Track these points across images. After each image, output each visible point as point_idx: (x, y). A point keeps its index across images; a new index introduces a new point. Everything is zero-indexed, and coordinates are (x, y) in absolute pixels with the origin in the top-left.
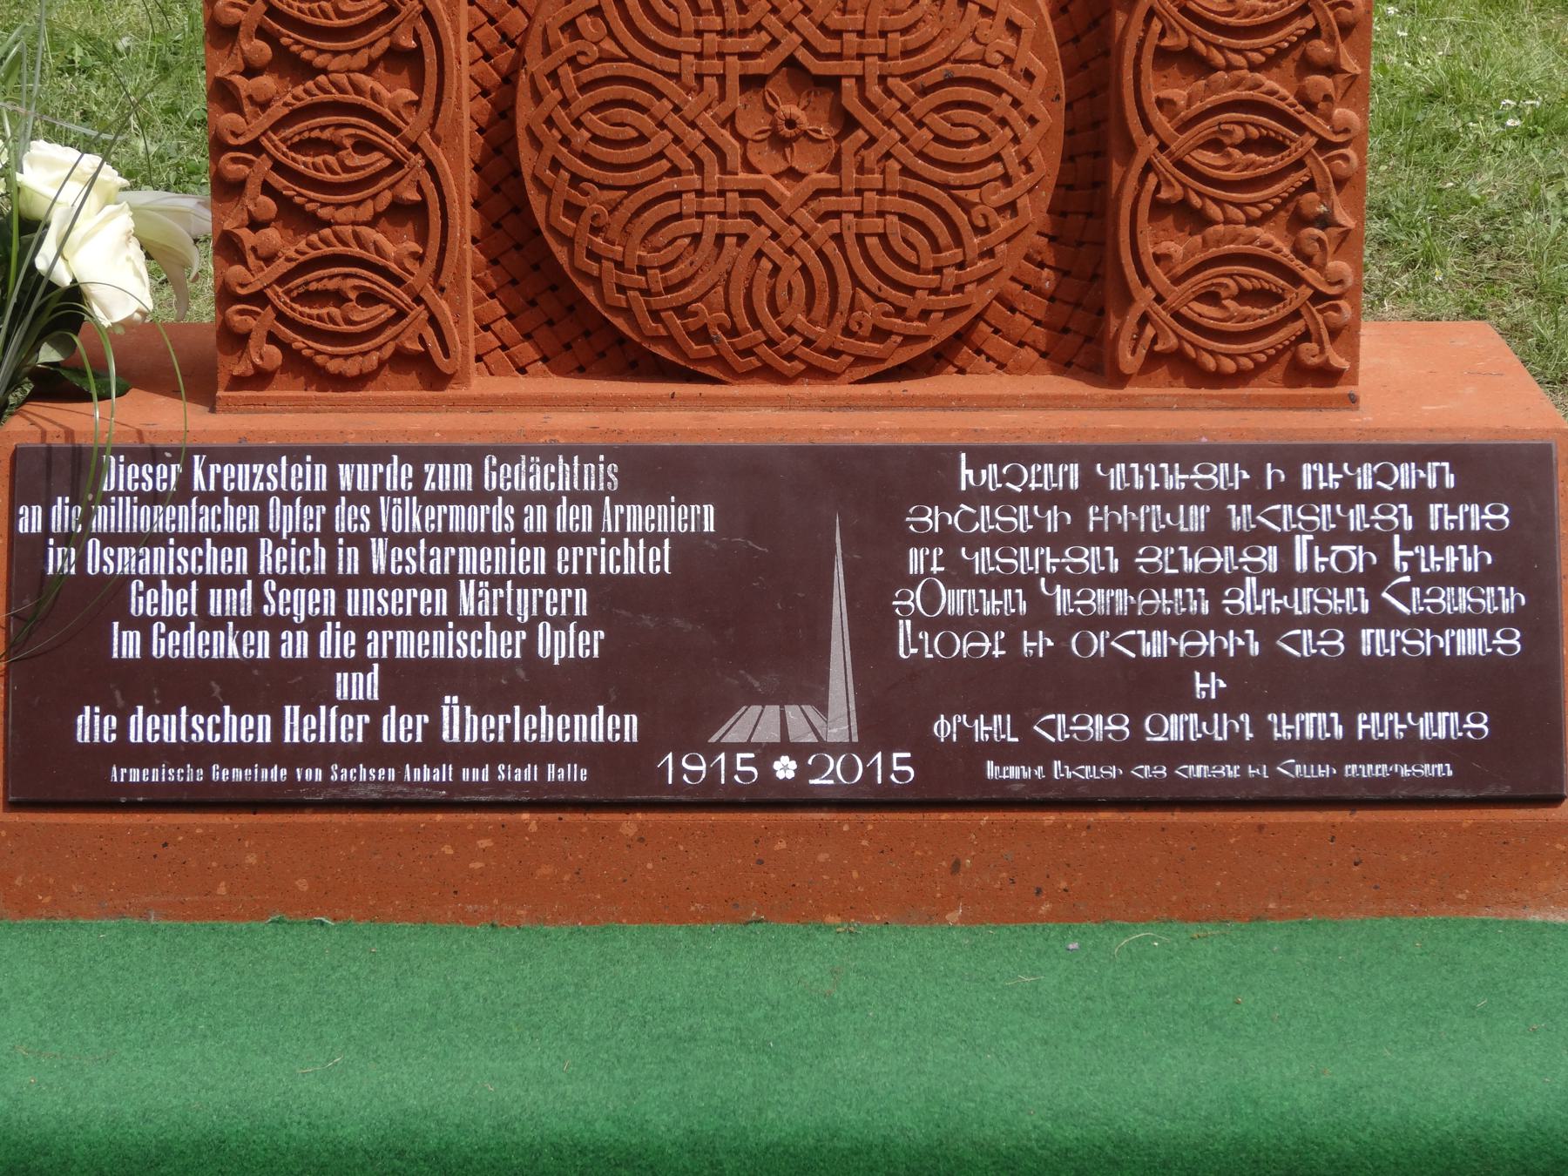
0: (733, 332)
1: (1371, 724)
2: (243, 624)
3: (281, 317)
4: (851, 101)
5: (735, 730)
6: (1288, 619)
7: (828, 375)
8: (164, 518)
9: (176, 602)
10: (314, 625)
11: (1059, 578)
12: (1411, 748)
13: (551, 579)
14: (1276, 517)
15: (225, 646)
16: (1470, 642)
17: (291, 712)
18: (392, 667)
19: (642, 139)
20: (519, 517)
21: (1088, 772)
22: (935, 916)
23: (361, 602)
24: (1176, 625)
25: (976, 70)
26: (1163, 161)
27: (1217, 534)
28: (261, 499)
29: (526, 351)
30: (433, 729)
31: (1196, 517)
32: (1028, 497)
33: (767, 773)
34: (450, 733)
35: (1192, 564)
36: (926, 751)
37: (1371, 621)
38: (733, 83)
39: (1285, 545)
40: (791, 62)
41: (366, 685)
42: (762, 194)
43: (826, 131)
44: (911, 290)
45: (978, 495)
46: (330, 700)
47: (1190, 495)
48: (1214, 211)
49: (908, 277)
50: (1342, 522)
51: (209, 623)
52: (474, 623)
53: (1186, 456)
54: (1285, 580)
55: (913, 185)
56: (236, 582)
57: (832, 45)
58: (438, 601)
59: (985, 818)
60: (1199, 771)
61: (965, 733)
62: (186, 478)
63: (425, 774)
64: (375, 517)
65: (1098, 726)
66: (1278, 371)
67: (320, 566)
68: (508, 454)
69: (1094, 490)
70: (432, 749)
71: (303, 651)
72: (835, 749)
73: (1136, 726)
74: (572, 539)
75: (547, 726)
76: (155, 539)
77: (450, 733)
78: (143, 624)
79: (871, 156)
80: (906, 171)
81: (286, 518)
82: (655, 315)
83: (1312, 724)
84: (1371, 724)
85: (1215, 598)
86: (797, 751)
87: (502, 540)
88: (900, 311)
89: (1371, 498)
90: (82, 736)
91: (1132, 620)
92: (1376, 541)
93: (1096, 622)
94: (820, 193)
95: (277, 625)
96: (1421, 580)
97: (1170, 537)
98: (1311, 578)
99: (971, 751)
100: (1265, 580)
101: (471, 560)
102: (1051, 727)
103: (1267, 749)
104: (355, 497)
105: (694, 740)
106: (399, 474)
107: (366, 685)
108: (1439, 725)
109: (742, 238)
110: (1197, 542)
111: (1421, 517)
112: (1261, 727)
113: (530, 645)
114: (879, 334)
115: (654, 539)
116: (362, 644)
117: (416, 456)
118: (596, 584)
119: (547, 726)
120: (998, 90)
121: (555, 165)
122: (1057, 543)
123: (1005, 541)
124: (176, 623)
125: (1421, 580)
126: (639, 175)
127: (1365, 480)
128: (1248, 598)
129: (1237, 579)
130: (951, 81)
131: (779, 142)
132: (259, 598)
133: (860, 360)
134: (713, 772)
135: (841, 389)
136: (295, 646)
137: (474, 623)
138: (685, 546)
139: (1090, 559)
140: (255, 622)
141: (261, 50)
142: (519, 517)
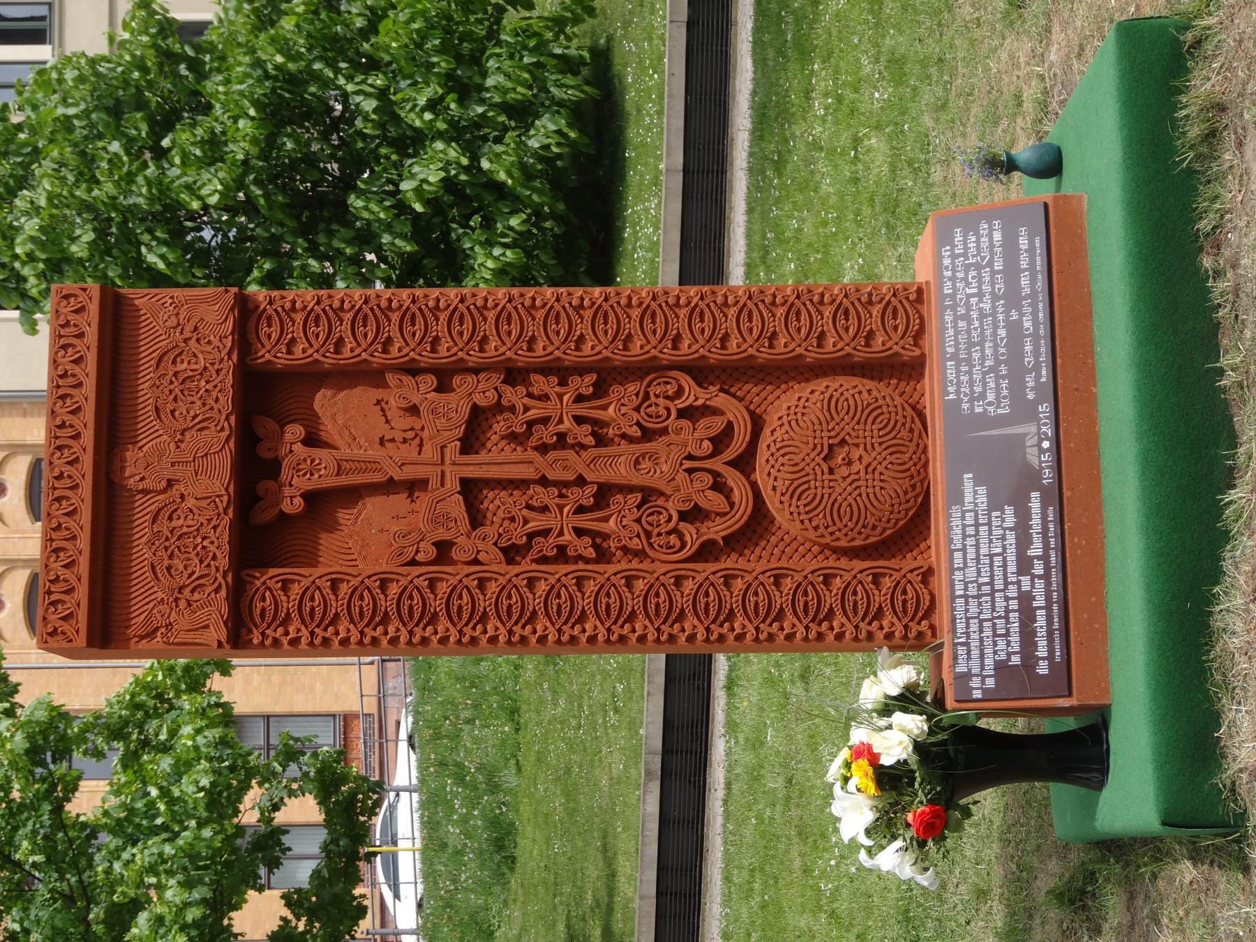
0: (912, 477)
1: (1024, 264)
2: (1008, 622)
3: (912, 620)
4: (836, 441)
5: (1034, 461)
6: (993, 293)
7: (926, 447)
8: (975, 653)
9: (1002, 644)
10: (1007, 599)
11: (982, 365)
13: (989, 524)
14: (961, 300)
15: (1015, 627)
16: (997, 236)
17: (1035, 604)
18: (1020, 572)
19: (850, 505)
20: (970, 536)
21: (1043, 349)
22: (1094, 396)
23: (999, 584)
24: (995, 326)
25: (826, 402)
26: (853, 344)
27: (967, 317)
28: (968, 619)
29: (923, 546)
31: (962, 324)
32: (958, 377)
33: (1048, 450)
34: (1039, 552)
35: (977, 324)
36: (1038, 401)
38: (831, 477)
39: (969, 296)
40: (825, 459)
42: (867, 468)
43: (846, 448)
44: (896, 421)
45: (958, 392)
46: (1031, 592)
47: (955, 327)
48: (868, 328)
49: (892, 422)
50: (962, 279)
51: (1007, 634)
52: (1004, 547)
54: (980, 295)
55: (863, 421)
56: (994, 624)
57: (819, 447)
58: (998, 561)
59: (1060, 381)
60: (1041, 315)
61: (1032, 389)
62: (962, 644)
63: (1053, 559)
64: (972, 582)
65: (1028, 348)
66: (919, 307)
67: (988, 598)
68: (951, 541)
69: (955, 357)
70: (1045, 558)
71: (1016, 602)
72: (1039, 429)
73: (1028, 336)
74: (976, 519)
75: (1036, 521)
76: (982, 651)
77: (1039, 552)
78: (1009, 654)
79: (853, 434)
80: (858, 423)
81: (973, 609)
82: (908, 501)
83: (1025, 282)
84: (1024, 264)
85: (986, 316)
86: (1041, 441)
87: (977, 541)
88: (904, 424)
89: (954, 271)
90: (1046, 672)
91: (995, 341)
92: (967, 268)
94: (866, 449)
95: (1007, 611)
96: (979, 253)
97: (968, 332)
98: (979, 287)
99: (1038, 387)
100: (981, 301)
101: (984, 550)
102: (1029, 363)
103: (1033, 295)
104: (966, 589)
105: (1038, 474)
106: (958, 576)
107: (1025, 580)
108: (1023, 243)
109: (881, 474)
110: (970, 323)
111: (959, 255)
113: (1011, 529)
114: (911, 430)
115: (975, 492)
116: (1012, 583)
117: (952, 570)
118: (989, 511)
119: (1036, 521)
120: (832, 396)
121: (860, 533)
122: (971, 366)
123: (971, 383)
125: (979, 253)
126: (862, 506)
127: (948, 274)
128: (987, 306)
129: (981, 310)
130: (829, 410)
131: (850, 463)
132: (999, 617)
133: (920, 436)
134: (1048, 467)
135: (930, 443)
136: (1014, 604)
137: (1004, 547)
139: (976, 356)
140: (1007, 618)
141: (825, 625)
142: (970, 536)
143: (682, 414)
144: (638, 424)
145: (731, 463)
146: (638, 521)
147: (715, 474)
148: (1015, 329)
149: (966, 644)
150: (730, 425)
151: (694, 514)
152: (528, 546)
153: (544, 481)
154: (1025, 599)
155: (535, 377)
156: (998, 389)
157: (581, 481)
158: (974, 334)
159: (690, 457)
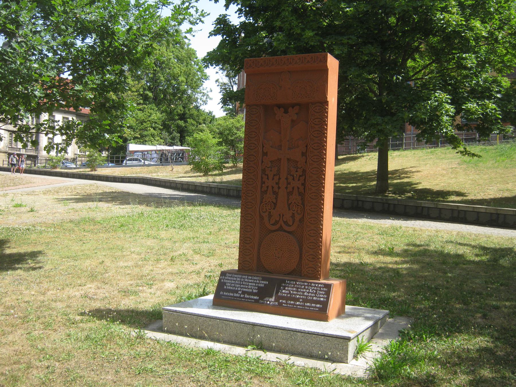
2: (233, 287)
5: (265, 299)
6: (308, 296)
8: (230, 278)
9: (229, 284)
10: (238, 287)
11: (292, 290)
12: (316, 307)
13: (255, 286)
15: (232, 288)
16: (322, 299)
23: (242, 286)
24: (299, 295)
27: (304, 288)
30: (244, 296)
35: (302, 290)
37: (315, 297)
41: (240, 292)
45: (287, 283)
47: (303, 285)
51: (231, 286)
52: (249, 289)
53: (303, 282)
54: (309, 293)
60: (299, 307)
65: (292, 302)
68: (254, 277)
69: (296, 284)
70: (244, 298)
74: (257, 283)
75: (252, 297)
76: (229, 280)
77: (245, 297)
81: (238, 279)
83: (308, 304)
84: (313, 305)
86: (269, 301)
89: (317, 287)
91: (296, 294)
93: (293, 294)
95: (236, 287)
98: (311, 293)
99: (282, 303)
101: (250, 284)
103: (304, 306)
106: (246, 277)
107: (240, 292)
108: (318, 306)
110: (302, 289)
111: (320, 289)
112: (304, 304)
115: (263, 284)
117: (248, 276)
118: (258, 287)
119: (252, 297)
124: (229, 286)
127: (317, 285)
128: (305, 294)
136: (236, 289)
137: (249, 289)
138: (265, 285)
140: (234, 287)
143: (293, 214)
144: (292, 203)
145: (281, 226)
146: (269, 202)
147: (279, 221)
148: (298, 300)
149: (231, 277)
150: (291, 226)
151: (270, 216)
152: (266, 175)
153: (279, 179)
154: (237, 292)
155: (304, 177)
156: (285, 293)
157: (279, 188)
158: (300, 290)
159: (283, 215)
